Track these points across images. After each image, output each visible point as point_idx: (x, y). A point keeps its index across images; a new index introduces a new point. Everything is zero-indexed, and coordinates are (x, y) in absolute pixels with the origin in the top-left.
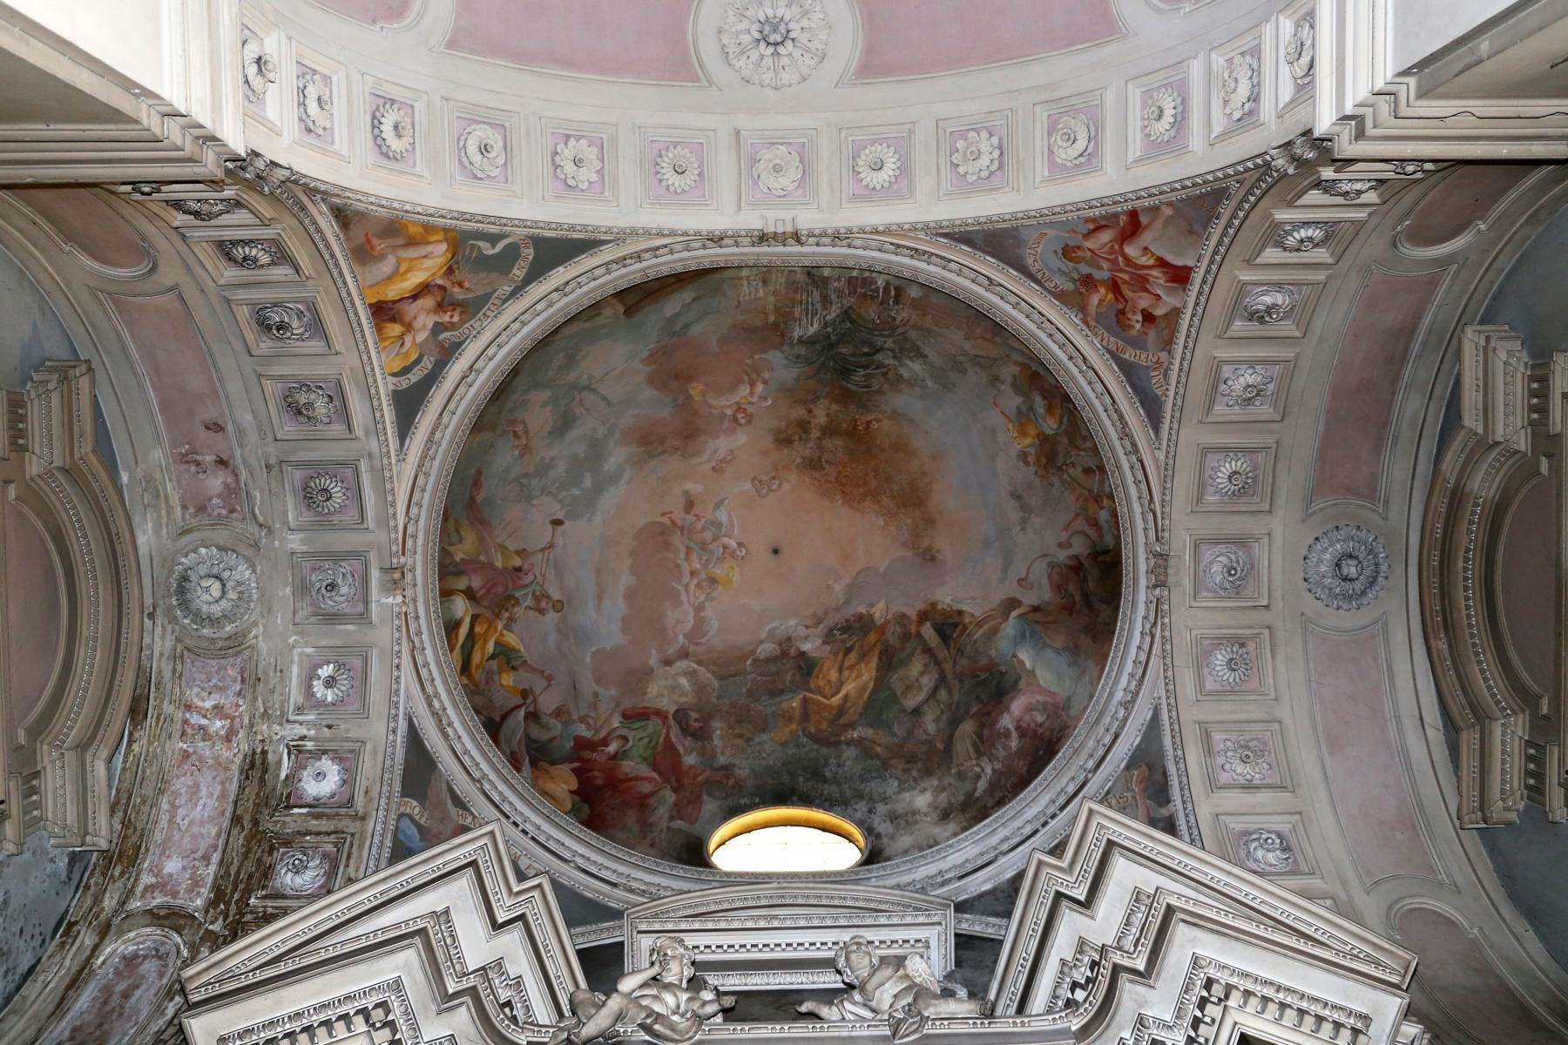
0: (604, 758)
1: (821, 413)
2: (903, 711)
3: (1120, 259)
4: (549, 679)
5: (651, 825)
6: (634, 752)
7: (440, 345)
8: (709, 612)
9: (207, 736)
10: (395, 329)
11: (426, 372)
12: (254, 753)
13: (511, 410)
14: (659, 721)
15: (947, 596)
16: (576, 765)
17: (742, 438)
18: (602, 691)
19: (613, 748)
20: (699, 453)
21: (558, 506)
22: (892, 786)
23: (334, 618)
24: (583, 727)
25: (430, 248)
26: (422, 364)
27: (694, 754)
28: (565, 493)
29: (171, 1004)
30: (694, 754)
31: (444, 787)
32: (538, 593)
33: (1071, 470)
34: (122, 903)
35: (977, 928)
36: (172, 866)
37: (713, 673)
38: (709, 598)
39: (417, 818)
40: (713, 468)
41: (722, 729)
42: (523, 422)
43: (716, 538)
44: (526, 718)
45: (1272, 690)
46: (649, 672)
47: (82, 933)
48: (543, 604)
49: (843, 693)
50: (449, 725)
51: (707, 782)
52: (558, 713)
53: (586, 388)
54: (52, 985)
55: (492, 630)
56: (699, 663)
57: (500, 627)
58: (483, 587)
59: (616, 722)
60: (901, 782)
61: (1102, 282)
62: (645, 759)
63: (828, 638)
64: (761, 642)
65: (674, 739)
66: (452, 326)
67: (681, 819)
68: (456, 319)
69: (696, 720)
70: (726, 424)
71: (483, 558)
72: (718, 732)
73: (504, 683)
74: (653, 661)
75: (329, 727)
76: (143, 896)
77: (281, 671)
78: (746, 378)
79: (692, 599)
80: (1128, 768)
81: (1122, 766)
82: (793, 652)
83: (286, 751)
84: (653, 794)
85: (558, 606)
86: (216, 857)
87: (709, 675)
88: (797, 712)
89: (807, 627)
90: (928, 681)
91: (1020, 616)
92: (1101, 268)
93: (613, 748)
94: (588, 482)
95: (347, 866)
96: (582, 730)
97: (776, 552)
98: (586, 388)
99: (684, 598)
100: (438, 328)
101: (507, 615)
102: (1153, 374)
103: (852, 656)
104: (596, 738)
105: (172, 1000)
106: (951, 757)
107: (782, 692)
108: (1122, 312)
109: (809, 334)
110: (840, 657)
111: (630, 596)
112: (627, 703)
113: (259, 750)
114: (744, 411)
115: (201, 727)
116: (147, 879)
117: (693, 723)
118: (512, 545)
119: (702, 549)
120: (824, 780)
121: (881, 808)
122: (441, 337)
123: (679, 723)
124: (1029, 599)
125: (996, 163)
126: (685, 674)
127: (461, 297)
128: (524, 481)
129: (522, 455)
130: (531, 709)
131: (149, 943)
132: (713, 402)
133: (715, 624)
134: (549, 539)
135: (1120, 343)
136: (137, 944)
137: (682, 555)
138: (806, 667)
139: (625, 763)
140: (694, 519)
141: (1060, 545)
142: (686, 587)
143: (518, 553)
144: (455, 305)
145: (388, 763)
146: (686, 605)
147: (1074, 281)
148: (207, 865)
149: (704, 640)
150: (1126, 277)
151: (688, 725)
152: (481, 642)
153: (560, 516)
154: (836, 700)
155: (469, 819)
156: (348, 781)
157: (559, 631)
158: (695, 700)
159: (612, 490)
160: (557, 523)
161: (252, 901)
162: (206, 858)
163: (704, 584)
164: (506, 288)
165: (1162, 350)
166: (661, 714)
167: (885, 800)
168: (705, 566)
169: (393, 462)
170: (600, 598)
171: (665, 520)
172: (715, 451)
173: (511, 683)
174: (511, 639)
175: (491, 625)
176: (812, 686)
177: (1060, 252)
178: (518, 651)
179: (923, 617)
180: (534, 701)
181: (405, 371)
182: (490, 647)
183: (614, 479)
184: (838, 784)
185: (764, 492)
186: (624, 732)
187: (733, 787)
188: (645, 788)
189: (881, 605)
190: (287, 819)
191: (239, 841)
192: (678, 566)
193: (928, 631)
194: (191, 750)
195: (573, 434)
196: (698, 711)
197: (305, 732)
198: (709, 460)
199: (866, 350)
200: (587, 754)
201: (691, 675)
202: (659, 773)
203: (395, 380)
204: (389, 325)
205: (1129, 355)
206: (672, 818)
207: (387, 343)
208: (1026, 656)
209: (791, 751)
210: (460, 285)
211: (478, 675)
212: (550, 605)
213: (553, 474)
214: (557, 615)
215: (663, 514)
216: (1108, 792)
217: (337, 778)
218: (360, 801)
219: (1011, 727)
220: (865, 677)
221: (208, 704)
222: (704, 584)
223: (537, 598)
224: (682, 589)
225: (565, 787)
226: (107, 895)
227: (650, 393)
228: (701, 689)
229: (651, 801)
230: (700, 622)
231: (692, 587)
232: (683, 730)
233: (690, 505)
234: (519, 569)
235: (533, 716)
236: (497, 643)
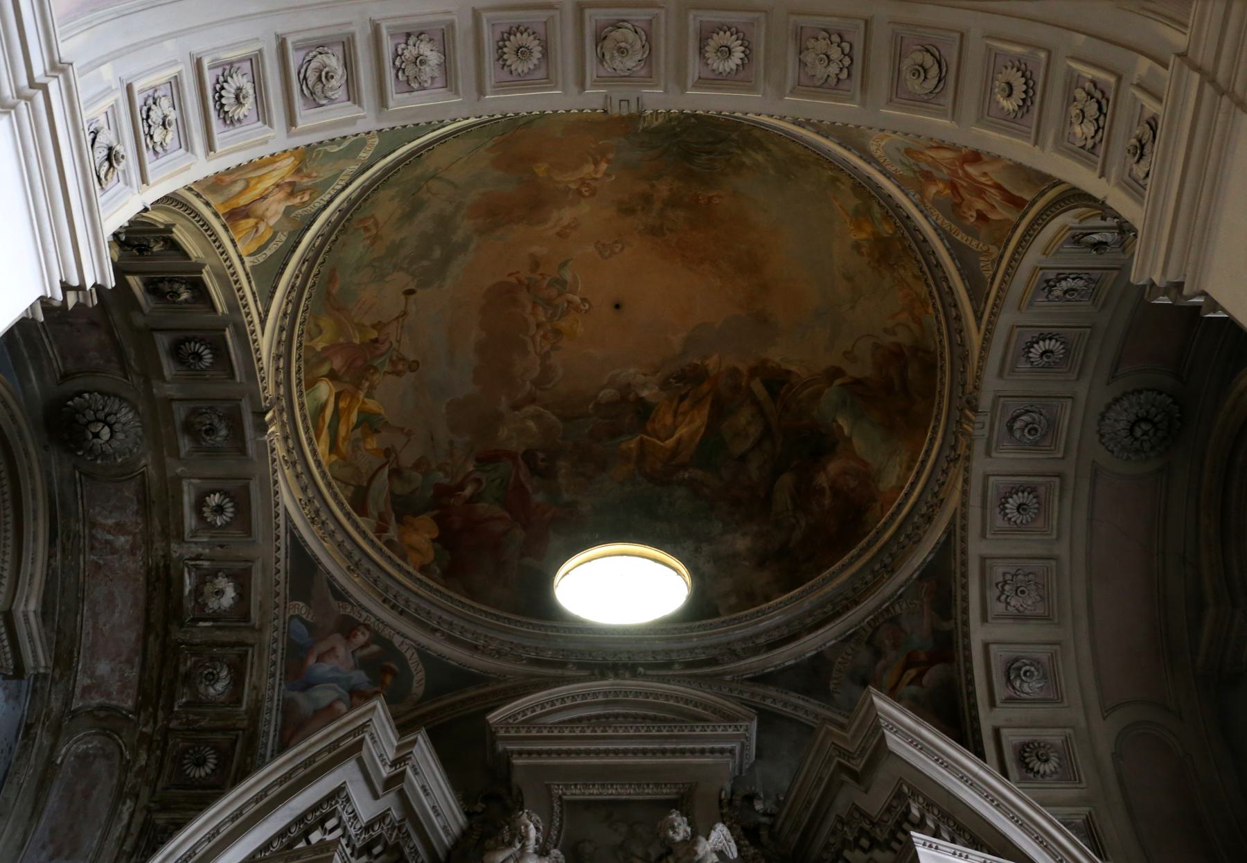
1: (664, 189)
3: (960, 171)
9: (114, 551)
11: (280, 244)
12: (158, 567)
15: (776, 355)
16: (435, 512)
17: (585, 208)
19: (468, 491)
23: (214, 452)
24: (441, 474)
25: (278, 164)
26: (277, 239)
29: (125, 808)
32: (394, 358)
33: (902, 271)
34: (67, 703)
35: (779, 706)
36: (103, 668)
39: (304, 617)
40: (558, 234)
42: (372, 216)
43: (560, 295)
44: (390, 476)
45: (1055, 532)
47: (39, 732)
48: (400, 367)
49: (677, 436)
52: (417, 466)
53: (433, 177)
54: (24, 785)
56: (546, 407)
59: (470, 467)
61: (942, 180)
63: (664, 385)
64: (603, 388)
65: (523, 479)
69: (543, 460)
70: (571, 197)
71: (341, 340)
72: (563, 471)
73: (369, 447)
75: (222, 546)
76: (82, 697)
77: (173, 497)
78: (590, 159)
80: (920, 578)
81: (915, 576)
82: (632, 397)
83: (186, 570)
85: (413, 366)
86: (137, 660)
87: (554, 418)
89: (645, 375)
90: (754, 431)
91: (842, 385)
92: (942, 171)
93: (468, 491)
95: (251, 675)
96: (440, 477)
97: (617, 306)
98: (433, 177)
99: (531, 348)
101: (367, 384)
102: (981, 258)
103: (686, 403)
105: (124, 803)
108: (959, 205)
109: (653, 126)
110: (675, 404)
113: (162, 564)
114: (588, 185)
115: (107, 542)
116: (83, 680)
117: (540, 463)
118: (367, 321)
124: (853, 371)
125: (845, 71)
127: (310, 183)
128: (376, 264)
129: (372, 244)
130: (394, 466)
131: (95, 743)
134: (403, 308)
135: (953, 226)
136: (86, 743)
138: (644, 411)
139: (479, 505)
140: (540, 277)
141: (886, 331)
142: (533, 338)
143: (374, 326)
147: (915, 172)
148: (133, 668)
149: (549, 386)
150: (964, 184)
152: (346, 413)
153: (412, 286)
154: (670, 443)
155: (349, 610)
156: (243, 594)
160: (410, 292)
161: (176, 709)
162: (129, 661)
165: (993, 244)
166: (511, 456)
171: (513, 280)
173: (375, 445)
174: (372, 405)
175: (354, 397)
176: (649, 428)
177: (903, 151)
178: (379, 414)
179: (753, 372)
180: (397, 458)
182: (354, 417)
185: (607, 254)
186: (477, 475)
189: (715, 358)
190: (194, 630)
191: (154, 646)
193: (757, 386)
194: (101, 562)
197: (200, 550)
199: (710, 139)
201: (538, 418)
203: (252, 258)
204: (243, 222)
205: (961, 237)
208: (844, 423)
210: (309, 176)
211: (344, 447)
214: (413, 374)
215: (510, 275)
216: (901, 596)
217: (233, 595)
218: (255, 614)
219: (826, 485)
220: (698, 423)
221: (110, 522)
223: (393, 362)
225: (427, 536)
226: (53, 697)
234: (376, 341)
236: (360, 412)
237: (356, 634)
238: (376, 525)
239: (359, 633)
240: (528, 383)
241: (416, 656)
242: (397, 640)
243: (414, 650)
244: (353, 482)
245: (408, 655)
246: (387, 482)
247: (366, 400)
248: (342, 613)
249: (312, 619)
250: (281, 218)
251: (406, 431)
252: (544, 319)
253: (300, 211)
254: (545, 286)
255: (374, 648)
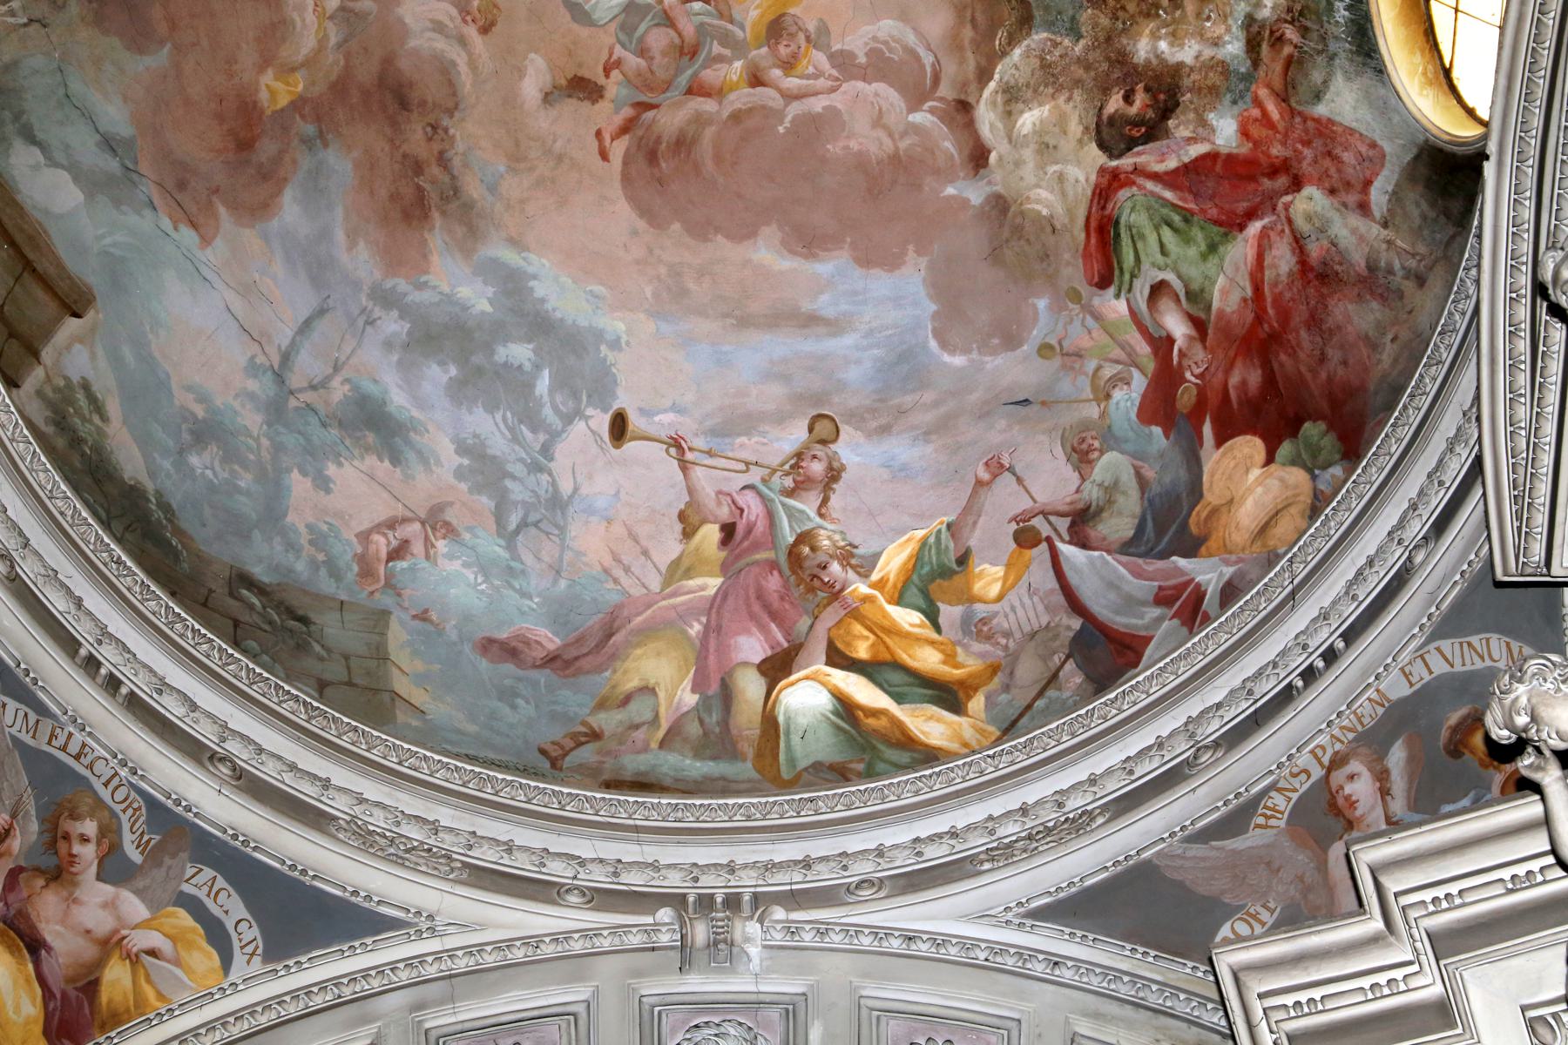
0: (1199, 354)
4: (997, 468)
5: (1372, 267)
6: (1195, 273)
7: (154, 856)
8: (857, 42)
10: (116, 978)
11: (221, 882)
13: (336, 574)
14: (1123, 194)
16: (1207, 430)
18: (1037, 334)
19: (1176, 326)
20: (446, 71)
21: (579, 426)
24: (1118, 395)
26: (202, 894)
27: (1211, 117)
28: (548, 412)
30: (1211, 117)
31: (1197, 850)
32: (789, 482)
37: (1012, 41)
38: (818, 40)
40: (485, 30)
41: (1155, 37)
42: (364, 537)
44: (1084, 545)
46: (1000, 205)
48: (817, 468)
50: (1060, 805)
51: (1283, 98)
52: (1081, 457)
53: (280, 378)
55: (866, 609)
56: (984, 75)
57: (863, 589)
58: (764, 629)
59: (1115, 306)
62: (1212, 248)
65: (1172, 164)
66: (109, 835)
67: (1368, 183)
68: (90, 827)
69: (1128, 99)
71: (695, 629)
72: (1163, 45)
73: (995, 590)
74: (975, 193)
79: (821, 83)
84: (1298, 242)
85: (824, 430)
93: (1176, 326)
94: (519, 352)
96: (1128, 398)
98: (280, 378)
99: (818, 105)
100: (114, 869)
101: (835, 567)
104: (1151, 366)
111: (808, 242)
112: (1073, 272)
117: (1133, 110)
118: (670, 547)
119: (694, 53)
122: (136, 856)
123: (1130, 144)
126: (1009, 115)
127: (34, 826)
128: (514, 520)
129: (450, 531)
130: (1063, 524)
132: (308, 44)
133: (887, 27)
137: (708, 106)
139: (1216, 304)
140: (615, 74)
142: (790, 97)
143: (688, 534)
144: (55, 837)
145: (1124, 990)
146: (837, 100)
149: (928, 59)
151: (1136, 122)
153: (602, 422)
155: (1278, 800)
157: (885, 430)
158: (1078, 95)
159: (539, 289)
160: (619, 428)
163: (783, 51)
164: (9, 719)
166: (1108, 185)
168: (739, 48)
169: (434, 945)
170: (811, 321)
171: (618, 149)
172: (439, 27)
173: (999, 571)
174: (893, 560)
178: (924, 543)
180: (1045, 514)
181: (218, 936)
182: (908, 618)
183: (512, 284)
187: (1304, 31)
188: (1282, 260)
192: (736, 117)
195: (398, 400)
196: (1106, 91)
198: (462, 41)
200: (1186, 397)
201: (1013, 97)
202: (1251, 215)
203: (239, 959)
206: (1364, 208)
207: (150, 993)
211: (969, 663)
212: (819, 450)
213: (499, 444)
214: (845, 430)
215: (604, 155)
222: (783, 51)
224: (795, 109)
225: (1256, 472)
227: (290, 211)
228: (1050, 77)
229: (1315, 250)
230: (879, 66)
231: (792, 83)
232: (1149, 138)
233: (582, 88)
234: (728, 531)
235: (1081, 522)
236: (899, 601)
237: (1348, 798)
238: (1176, 622)
239: (1348, 789)
240: (918, 117)
241: (1445, 645)
242: (1397, 688)
243: (1431, 647)
244: (1057, 660)
245: (1440, 667)
246: (1096, 553)
247: (875, 576)
248: (1282, 824)
249: (1272, 912)
250: (137, 892)
251: (985, 476)
252: (738, 64)
253: (128, 839)
254: (642, 62)
255: (1397, 756)
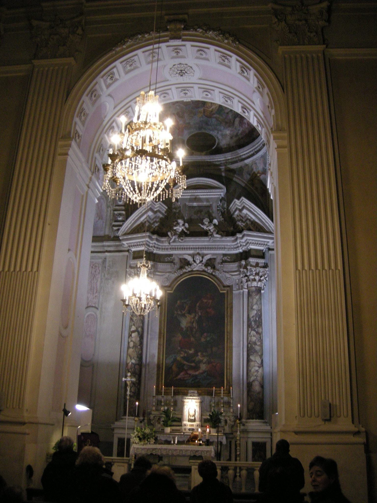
2: (225, 113)
22: (222, 128)
60: (224, 127)
87: (183, 105)
88: (202, 112)
106: (234, 124)
107: (199, 108)
120: (209, 125)
121: (220, 133)
154: (211, 109)
167: (221, 131)
184: (211, 126)
209: (202, 119)
